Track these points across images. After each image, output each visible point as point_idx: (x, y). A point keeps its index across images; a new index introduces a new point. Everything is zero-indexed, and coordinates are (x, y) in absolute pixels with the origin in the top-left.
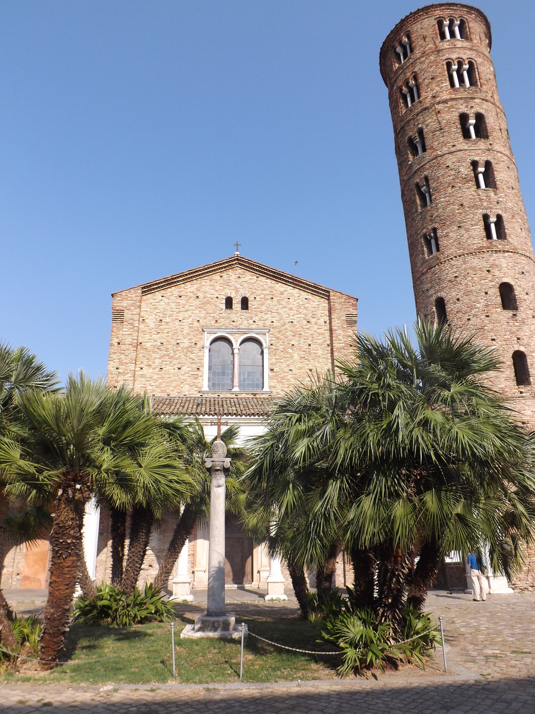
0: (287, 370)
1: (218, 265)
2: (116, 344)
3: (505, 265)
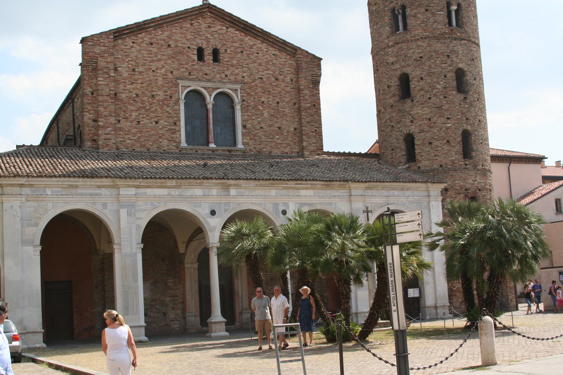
0: (258, 127)
1: (190, 12)
2: (90, 94)
3: (461, 52)
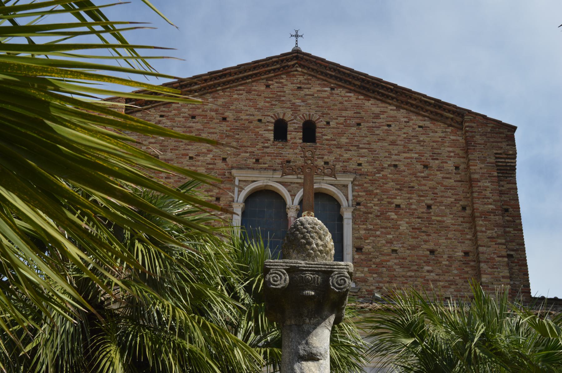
1: (263, 66)
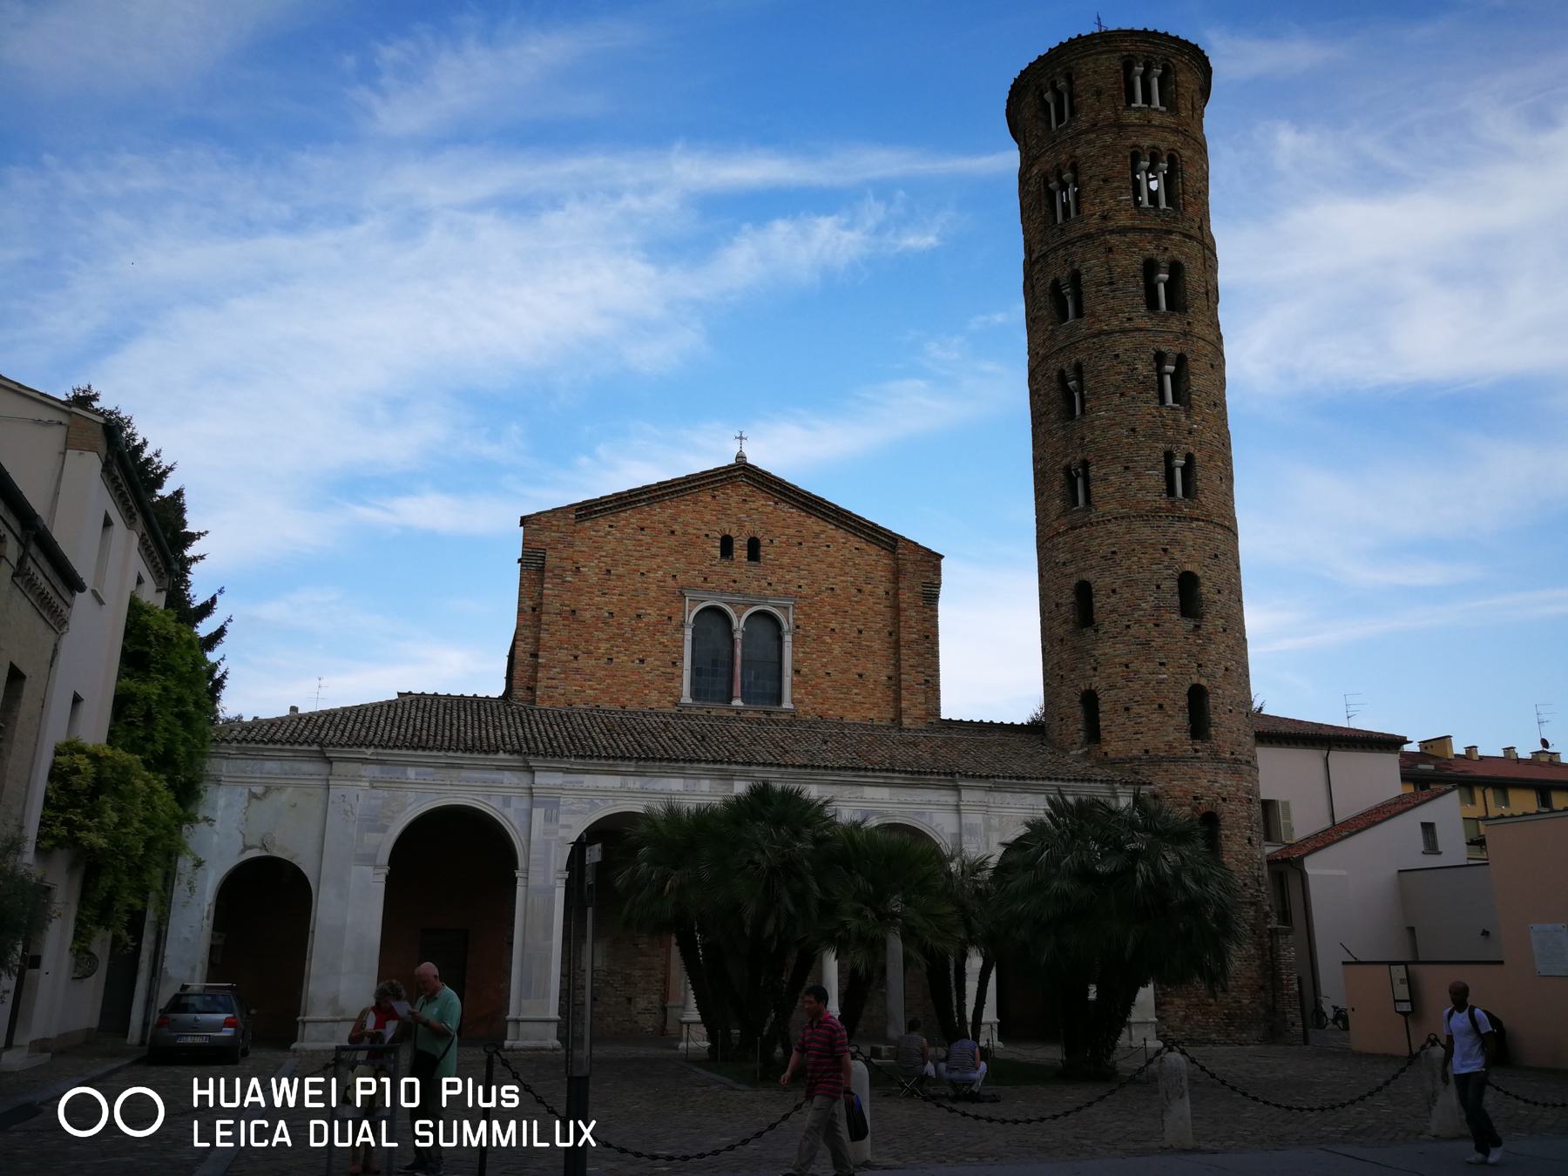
0: (821, 673)
